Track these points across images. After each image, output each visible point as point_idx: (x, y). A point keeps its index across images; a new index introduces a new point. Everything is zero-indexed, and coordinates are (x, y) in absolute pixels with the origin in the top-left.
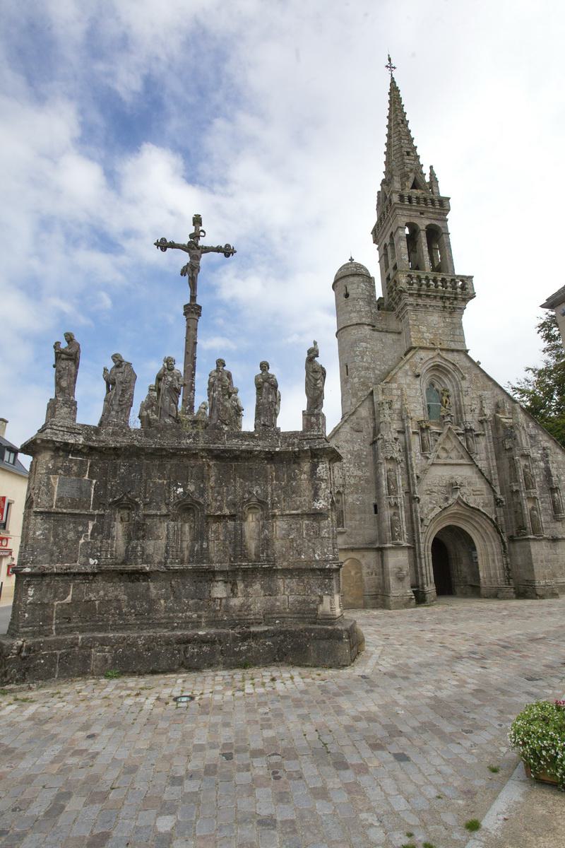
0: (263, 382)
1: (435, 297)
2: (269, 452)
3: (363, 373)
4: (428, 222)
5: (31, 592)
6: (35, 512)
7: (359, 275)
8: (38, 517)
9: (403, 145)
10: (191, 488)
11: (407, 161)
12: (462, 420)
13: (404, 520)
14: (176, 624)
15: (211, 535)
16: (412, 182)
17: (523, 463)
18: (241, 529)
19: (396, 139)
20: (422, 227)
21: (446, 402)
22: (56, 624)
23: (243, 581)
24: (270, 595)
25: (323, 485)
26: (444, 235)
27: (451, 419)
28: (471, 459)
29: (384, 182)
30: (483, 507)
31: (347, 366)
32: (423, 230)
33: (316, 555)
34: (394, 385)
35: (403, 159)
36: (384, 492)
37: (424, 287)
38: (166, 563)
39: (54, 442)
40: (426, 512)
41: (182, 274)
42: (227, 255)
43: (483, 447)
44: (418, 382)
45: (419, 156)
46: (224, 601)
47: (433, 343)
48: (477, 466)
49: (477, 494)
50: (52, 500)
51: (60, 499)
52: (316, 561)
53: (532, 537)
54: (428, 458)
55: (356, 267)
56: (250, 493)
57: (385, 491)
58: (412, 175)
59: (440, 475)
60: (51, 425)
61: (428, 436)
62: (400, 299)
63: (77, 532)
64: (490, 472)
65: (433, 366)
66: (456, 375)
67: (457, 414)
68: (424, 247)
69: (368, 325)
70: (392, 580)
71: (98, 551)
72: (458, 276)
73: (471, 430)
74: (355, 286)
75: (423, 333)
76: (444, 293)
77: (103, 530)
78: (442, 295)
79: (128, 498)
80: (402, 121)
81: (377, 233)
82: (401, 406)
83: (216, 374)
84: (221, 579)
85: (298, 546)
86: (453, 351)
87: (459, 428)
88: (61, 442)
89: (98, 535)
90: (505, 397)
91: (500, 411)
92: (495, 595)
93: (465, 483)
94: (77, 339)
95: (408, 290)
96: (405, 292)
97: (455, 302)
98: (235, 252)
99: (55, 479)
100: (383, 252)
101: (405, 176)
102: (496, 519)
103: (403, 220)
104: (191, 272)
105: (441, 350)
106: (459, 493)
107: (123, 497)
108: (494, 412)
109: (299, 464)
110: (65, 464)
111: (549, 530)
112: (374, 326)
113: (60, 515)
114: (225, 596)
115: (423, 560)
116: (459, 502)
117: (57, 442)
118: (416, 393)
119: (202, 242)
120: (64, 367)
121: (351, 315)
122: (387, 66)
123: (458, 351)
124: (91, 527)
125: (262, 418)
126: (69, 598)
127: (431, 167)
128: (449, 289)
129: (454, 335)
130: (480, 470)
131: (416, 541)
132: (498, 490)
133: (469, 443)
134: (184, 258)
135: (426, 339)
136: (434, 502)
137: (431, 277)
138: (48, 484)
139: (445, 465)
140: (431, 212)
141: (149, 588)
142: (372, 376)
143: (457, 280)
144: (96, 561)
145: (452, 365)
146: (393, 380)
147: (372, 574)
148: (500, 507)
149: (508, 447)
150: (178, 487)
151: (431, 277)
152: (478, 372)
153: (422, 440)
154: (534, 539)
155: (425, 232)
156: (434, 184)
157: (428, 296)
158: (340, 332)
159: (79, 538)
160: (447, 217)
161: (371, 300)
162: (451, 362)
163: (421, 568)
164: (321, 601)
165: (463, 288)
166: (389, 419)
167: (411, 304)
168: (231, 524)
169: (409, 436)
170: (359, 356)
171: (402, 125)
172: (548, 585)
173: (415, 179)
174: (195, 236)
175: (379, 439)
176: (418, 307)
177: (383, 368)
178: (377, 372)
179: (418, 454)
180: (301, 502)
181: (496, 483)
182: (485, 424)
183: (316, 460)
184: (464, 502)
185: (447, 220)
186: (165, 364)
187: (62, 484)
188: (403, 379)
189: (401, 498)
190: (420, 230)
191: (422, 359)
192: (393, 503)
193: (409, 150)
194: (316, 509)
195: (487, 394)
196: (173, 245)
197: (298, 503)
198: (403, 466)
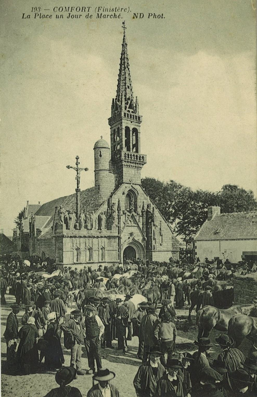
20: (131, 129)
116: (133, 239)
151: (132, 154)
195: (145, 201)
196: (71, 167)
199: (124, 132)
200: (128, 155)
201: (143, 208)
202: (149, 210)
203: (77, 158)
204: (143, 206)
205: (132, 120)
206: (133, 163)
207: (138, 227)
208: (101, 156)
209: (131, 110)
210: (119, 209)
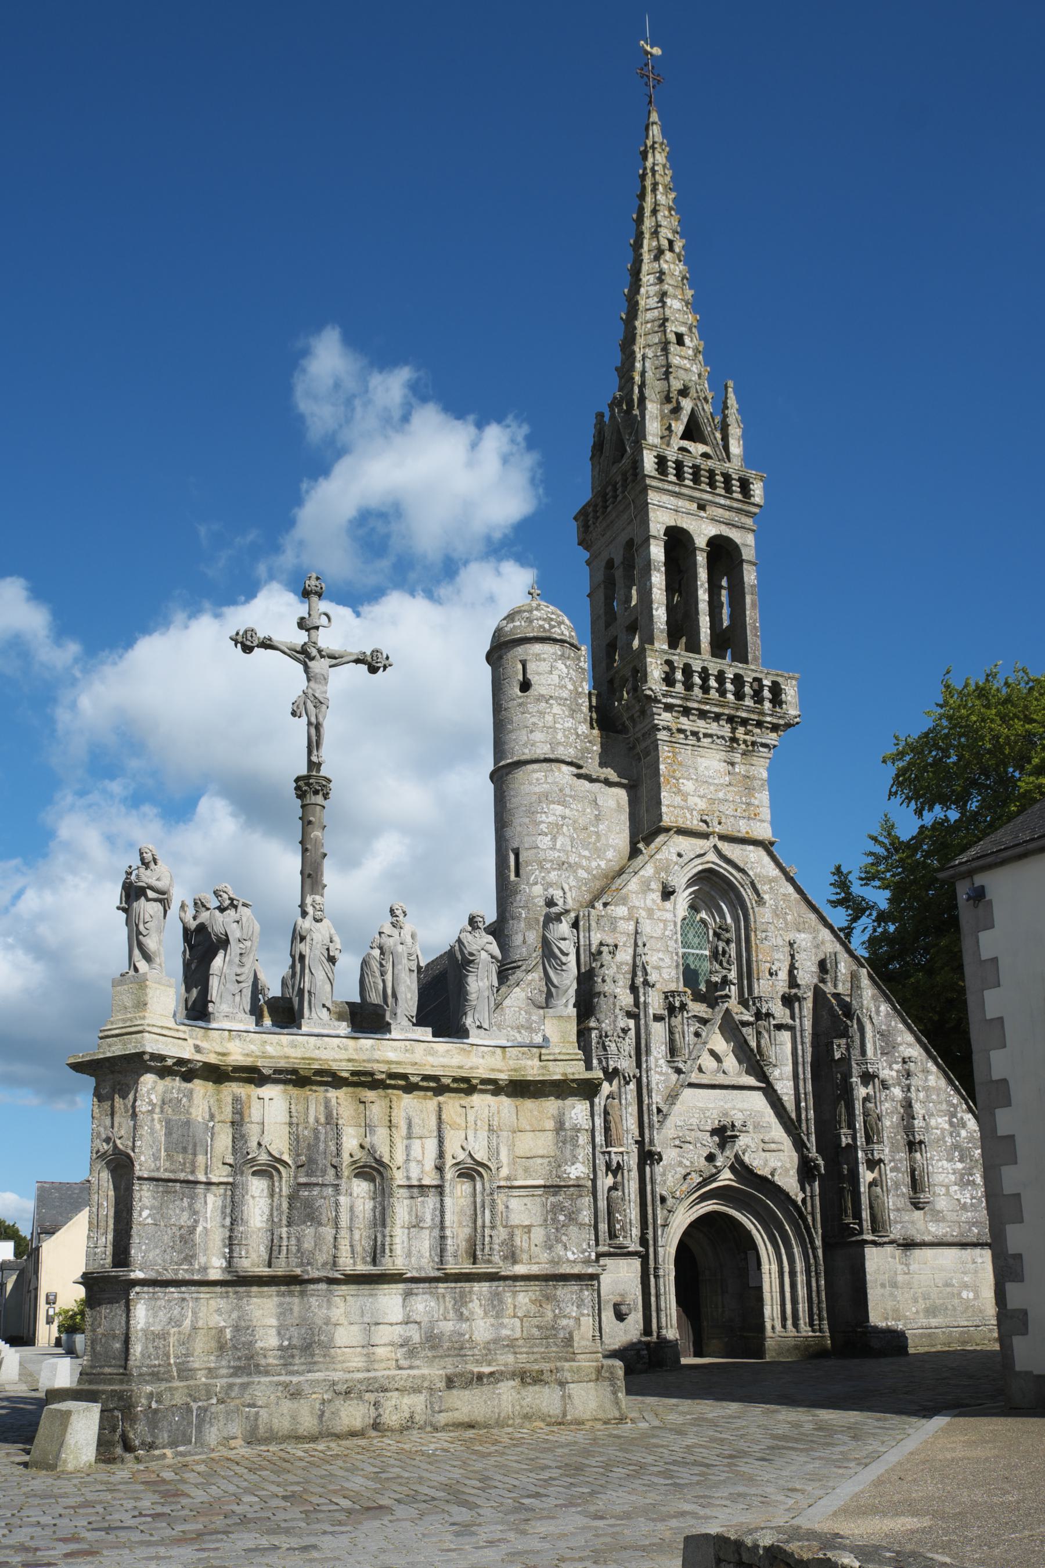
4: (712, 530)
7: (555, 641)
16: (685, 420)
20: (701, 542)
21: (724, 952)
32: (702, 550)
34: (621, 911)
54: (679, 1071)
59: (695, 1111)
66: (748, 895)
68: (700, 592)
73: (769, 1015)
74: (544, 666)
78: (733, 712)
91: (828, 977)
93: (750, 1128)
95: (664, 696)
96: (659, 702)
97: (757, 731)
108: (815, 980)
118: (665, 929)
121: (532, 736)
128: (748, 702)
133: (763, 1042)
135: (691, 810)
137: (713, 670)
140: (722, 506)
151: (713, 670)
152: (791, 889)
153: (671, 1033)
155: (705, 555)
157: (703, 715)
167: (668, 729)
169: (646, 1025)
170: (546, 835)
173: (693, 415)
182: (797, 1005)
188: (639, 893)
195: (803, 939)
199: (657, 552)
200: (687, 670)
201: (793, 982)
202: (828, 988)
204: (792, 968)
206: (717, 717)
208: (525, 686)
209: (697, 449)
210: (640, 980)
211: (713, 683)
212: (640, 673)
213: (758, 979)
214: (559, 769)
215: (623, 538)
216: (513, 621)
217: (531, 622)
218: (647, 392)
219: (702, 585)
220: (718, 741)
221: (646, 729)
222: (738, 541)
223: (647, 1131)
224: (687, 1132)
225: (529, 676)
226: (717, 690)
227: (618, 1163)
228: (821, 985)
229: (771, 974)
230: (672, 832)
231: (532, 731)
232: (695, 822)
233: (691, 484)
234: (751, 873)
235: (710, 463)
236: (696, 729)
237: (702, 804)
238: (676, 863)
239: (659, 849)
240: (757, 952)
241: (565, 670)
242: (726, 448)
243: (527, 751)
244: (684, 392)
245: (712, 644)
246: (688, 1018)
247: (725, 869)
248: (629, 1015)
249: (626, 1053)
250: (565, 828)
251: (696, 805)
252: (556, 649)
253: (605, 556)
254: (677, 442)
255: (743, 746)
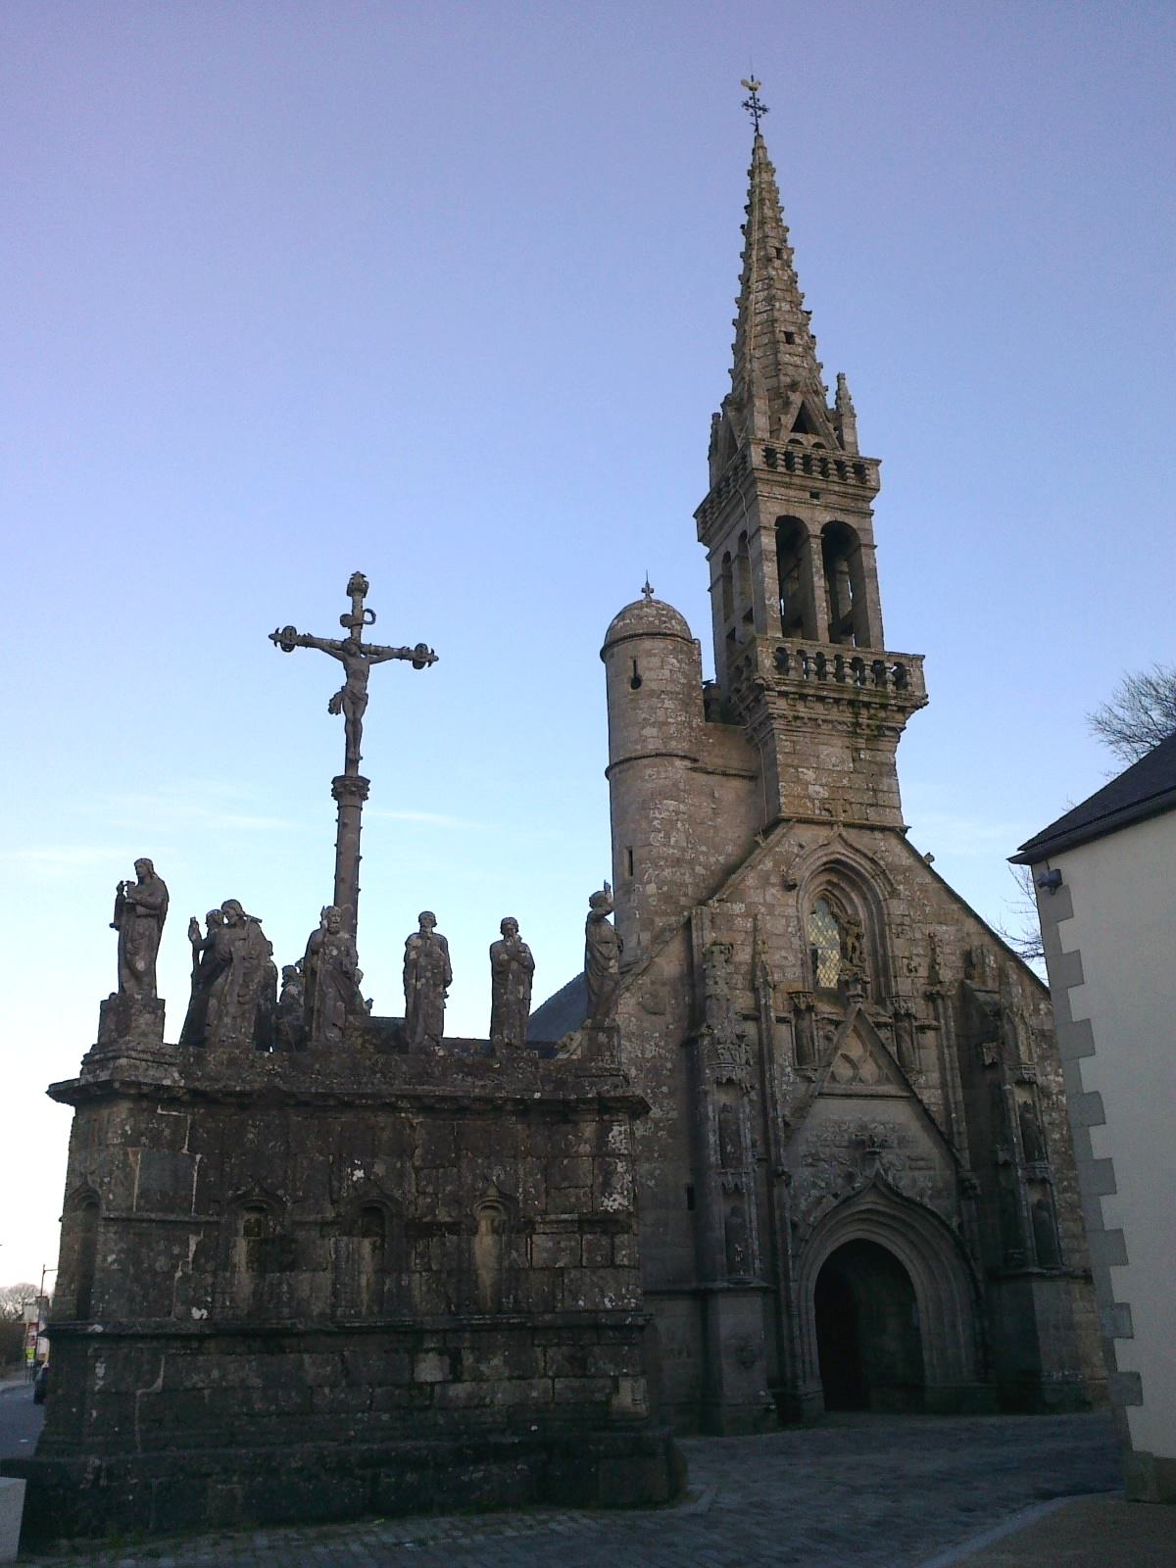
0: (509, 961)
1: (837, 701)
2: (522, 1101)
3: (667, 872)
4: (827, 517)
5: (100, 1370)
6: (107, 1219)
8: (113, 1229)
9: (776, 314)
10: (379, 1169)
11: (787, 358)
12: (889, 992)
13: (755, 1224)
14: (352, 1433)
15: (415, 1262)
16: (796, 414)
17: (1021, 1096)
18: (470, 1249)
19: (761, 295)
20: (815, 529)
21: (854, 948)
22: (141, 1430)
23: (472, 1349)
24: (520, 1378)
25: (621, 1167)
26: (863, 550)
27: (864, 989)
28: (906, 1084)
29: (727, 402)
30: (931, 1197)
31: (631, 853)
32: (816, 537)
33: (606, 1300)
34: (738, 908)
35: (776, 352)
36: (713, 1159)
37: (813, 678)
38: (333, 1314)
39: (139, 1084)
40: (803, 1206)
41: (331, 711)
42: (418, 665)
43: (930, 1056)
44: (792, 901)
45: (821, 366)
46: (437, 1388)
47: (827, 810)
48: (920, 1102)
49: (919, 1167)
50: (131, 1195)
51: (142, 1195)
52: (607, 1311)
53: (1036, 1270)
54: (809, 1080)
55: (659, 616)
56: (486, 1179)
57: (714, 1158)
58: (796, 399)
60: (128, 1049)
61: (810, 1027)
62: (757, 700)
63: (172, 1257)
64: (949, 1121)
65: (825, 864)
66: (879, 886)
67: (877, 977)
68: (816, 579)
69: (684, 757)
70: (727, 1366)
71: (206, 1294)
72: (891, 654)
73: (908, 1015)
74: (655, 661)
75: (808, 783)
76: (858, 694)
77: (215, 1256)
79: (262, 1189)
80: (779, 251)
81: (711, 519)
82: (753, 957)
83: (419, 942)
84: (433, 1345)
85: (571, 1280)
86: (872, 828)
87: (882, 1012)
88: (151, 1084)
89: (206, 1263)
90: (987, 939)
92: (956, 1404)
93: (893, 1140)
94: (160, 871)
95: (777, 684)
97: (882, 714)
98: (437, 659)
99: (135, 1154)
100: (720, 571)
101: (779, 398)
102: (960, 1226)
103: (770, 511)
104: (350, 703)
105: (846, 825)
106: (878, 1164)
107: (253, 1189)
108: (961, 976)
109: (576, 1123)
110: (151, 1126)
111: (1078, 1256)
112: (695, 760)
113: (144, 1225)
114: (439, 1378)
115: (796, 1321)
117: (146, 1084)
119: (369, 636)
120: (141, 931)
122: (746, 104)
123: (883, 829)
124: (193, 1247)
125: (505, 1032)
126: (160, 1381)
127: (840, 378)
128: (869, 685)
129: (874, 790)
130: (926, 1111)
131: (781, 1276)
132: (965, 1157)
134: (333, 675)
135: (812, 800)
136: (823, 1185)
138: (125, 1164)
139: (849, 1096)
141: (301, 1364)
142: (688, 879)
143: (887, 665)
144: (205, 1312)
145: (871, 871)
146: (737, 896)
147: (680, 1353)
148: (970, 1198)
149: (988, 1061)
150: (355, 1167)
152: (928, 879)
153: (798, 1037)
154: (1041, 1276)
155: (820, 541)
156: (846, 420)
157: (821, 699)
158: (617, 770)
159: (175, 1267)
160: (873, 505)
161: (689, 695)
162: (865, 856)
163: (792, 1340)
164: (616, 1389)
165: (901, 679)
166: (726, 990)
167: (784, 717)
168: (451, 1239)
169: (769, 1029)
170: (660, 832)
171: (777, 263)
172: (1068, 1383)
174: (352, 621)
175: (702, 1035)
176: (799, 723)
177: (712, 860)
178: (699, 869)
179: (789, 1069)
180: (578, 1198)
181: (962, 1142)
182: (940, 1002)
183: (606, 1117)
184: (887, 1185)
185: (871, 514)
186: (325, 922)
187: (146, 1166)
188: (758, 890)
189: (750, 1176)
190: (809, 536)
191: (801, 846)
192: (732, 1186)
193: (792, 329)
194: (606, 1211)
195: (945, 932)
196: (308, 642)
197: (573, 1200)
198: (755, 1098)
199: (768, 542)
202: (973, 984)
203: (357, 587)
205: (818, 484)
206: (837, 701)
207: (914, 1099)
211: (830, 668)
212: (751, 663)
213: (895, 977)
214: (672, 765)
215: (738, 531)
216: (624, 619)
217: (641, 618)
218: (754, 390)
219: (818, 572)
220: (840, 727)
221: (761, 719)
222: (855, 526)
223: (773, 1148)
224: (820, 1149)
225: (639, 672)
226: (835, 675)
227: (736, 1185)
228: (968, 982)
229: (910, 971)
230: (791, 823)
231: (643, 728)
232: (817, 812)
233: (802, 474)
234: (882, 863)
235: (821, 452)
236: (814, 716)
237: (824, 793)
238: (797, 855)
239: (779, 842)
240: (892, 946)
241: (678, 665)
242: (840, 438)
243: (639, 747)
244: (793, 386)
245: (830, 627)
246: (817, 1021)
247: (854, 860)
248: (746, 1018)
249: (743, 1062)
250: (679, 825)
251: (818, 793)
252: (669, 644)
253: (722, 551)
254: (786, 435)
255: (867, 732)
